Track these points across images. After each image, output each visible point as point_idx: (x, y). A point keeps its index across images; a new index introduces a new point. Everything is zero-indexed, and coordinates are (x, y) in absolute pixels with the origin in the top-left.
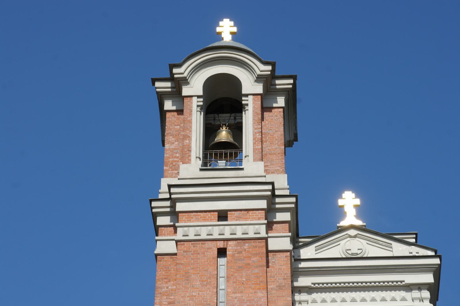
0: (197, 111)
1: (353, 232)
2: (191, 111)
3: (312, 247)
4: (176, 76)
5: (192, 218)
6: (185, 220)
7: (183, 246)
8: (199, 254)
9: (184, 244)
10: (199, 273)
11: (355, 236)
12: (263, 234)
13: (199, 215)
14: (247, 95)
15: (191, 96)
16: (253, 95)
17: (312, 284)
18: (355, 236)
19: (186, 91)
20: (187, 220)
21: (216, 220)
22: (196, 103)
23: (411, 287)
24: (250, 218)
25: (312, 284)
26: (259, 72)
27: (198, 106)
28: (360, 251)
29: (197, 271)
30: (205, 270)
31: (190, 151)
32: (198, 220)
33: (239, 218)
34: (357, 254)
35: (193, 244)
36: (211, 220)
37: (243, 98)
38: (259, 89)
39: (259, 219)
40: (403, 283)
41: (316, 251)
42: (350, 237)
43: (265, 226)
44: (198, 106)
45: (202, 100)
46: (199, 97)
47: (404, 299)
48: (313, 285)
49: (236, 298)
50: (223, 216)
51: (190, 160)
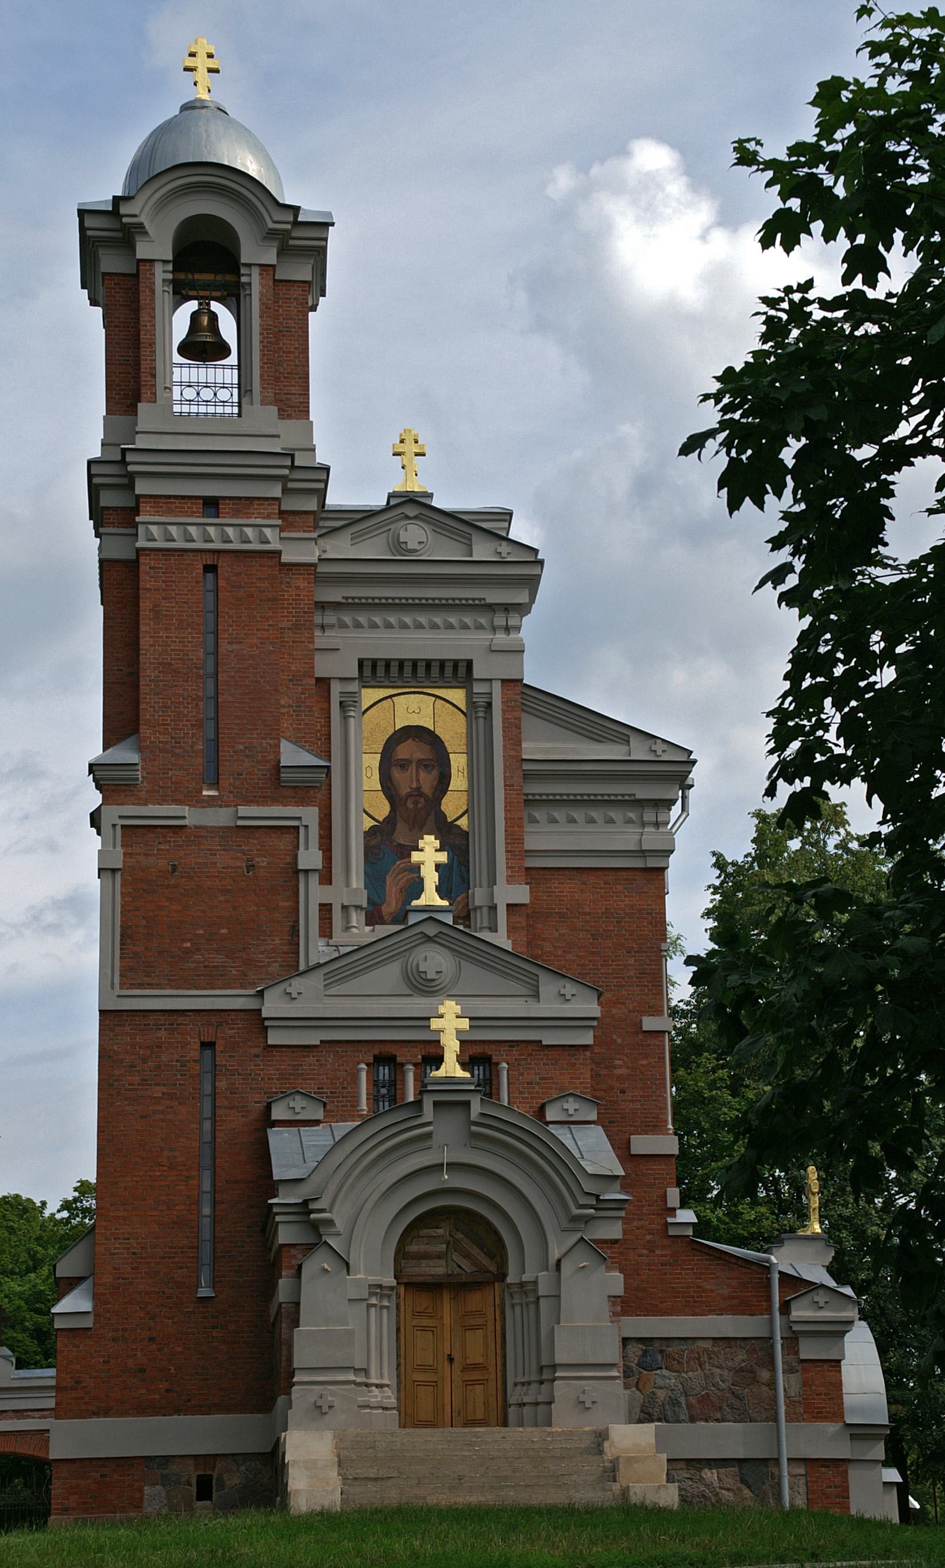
0: (164, 291)
1: (411, 511)
2: (153, 292)
3: (347, 535)
4: (125, 220)
5: (162, 507)
6: (150, 511)
7: (148, 558)
8: (174, 573)
9: (150, 555)
10: (174, 607)
11: (416, 517)
12: (274, 545)
13: (171, 503)
14: (249, 265)
15: (152, 261)
16: (260, 265)
17: (343, 598)
18: (416, 517)
19: (143, 250)
20: (154, 512)
21: (200, 513)
22: (161, 275)
23: (494, 607)
24: (254, 514)
25: (343, 598)
26: (271, 225)
27: (164, 280)
28: (422, 546)
29: (172, 603)
30: (184, 602)
31: (154, 376)
32: (169, 512)
33: (236, 514)
34: (416, 551)
35: (166, 555)
36: (192, 514)
37: (243, 271)
38: (270, 257)
39: (269, 517)
40: (483, 602)
41: (352, 539)
42: (408, 517)
43: (278, 530)
44: (164, 280)
45: (170, 267)
46: (165, 262)
47: (480, 627)
48: (344, 601)
49: (232, 651)
50: (211, 505)
51: (155, 394)
